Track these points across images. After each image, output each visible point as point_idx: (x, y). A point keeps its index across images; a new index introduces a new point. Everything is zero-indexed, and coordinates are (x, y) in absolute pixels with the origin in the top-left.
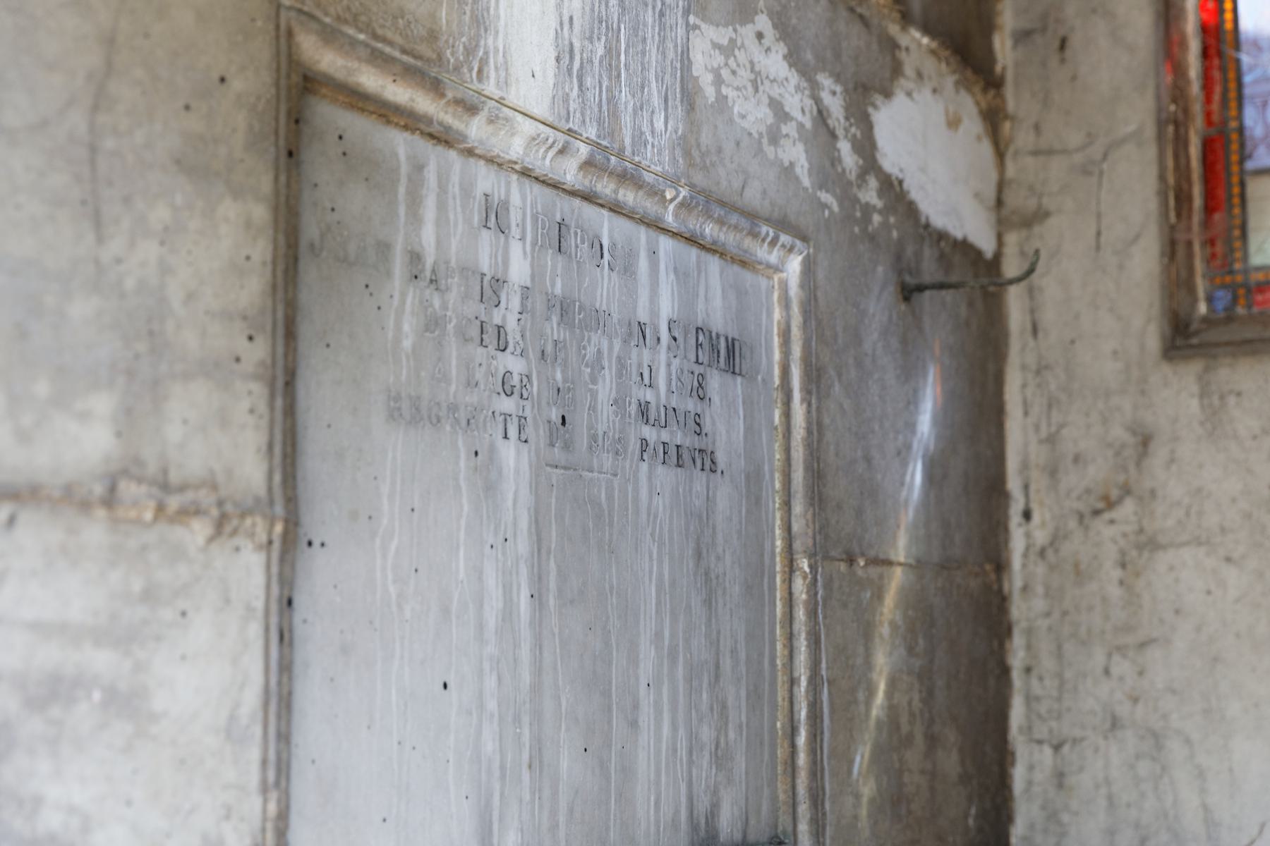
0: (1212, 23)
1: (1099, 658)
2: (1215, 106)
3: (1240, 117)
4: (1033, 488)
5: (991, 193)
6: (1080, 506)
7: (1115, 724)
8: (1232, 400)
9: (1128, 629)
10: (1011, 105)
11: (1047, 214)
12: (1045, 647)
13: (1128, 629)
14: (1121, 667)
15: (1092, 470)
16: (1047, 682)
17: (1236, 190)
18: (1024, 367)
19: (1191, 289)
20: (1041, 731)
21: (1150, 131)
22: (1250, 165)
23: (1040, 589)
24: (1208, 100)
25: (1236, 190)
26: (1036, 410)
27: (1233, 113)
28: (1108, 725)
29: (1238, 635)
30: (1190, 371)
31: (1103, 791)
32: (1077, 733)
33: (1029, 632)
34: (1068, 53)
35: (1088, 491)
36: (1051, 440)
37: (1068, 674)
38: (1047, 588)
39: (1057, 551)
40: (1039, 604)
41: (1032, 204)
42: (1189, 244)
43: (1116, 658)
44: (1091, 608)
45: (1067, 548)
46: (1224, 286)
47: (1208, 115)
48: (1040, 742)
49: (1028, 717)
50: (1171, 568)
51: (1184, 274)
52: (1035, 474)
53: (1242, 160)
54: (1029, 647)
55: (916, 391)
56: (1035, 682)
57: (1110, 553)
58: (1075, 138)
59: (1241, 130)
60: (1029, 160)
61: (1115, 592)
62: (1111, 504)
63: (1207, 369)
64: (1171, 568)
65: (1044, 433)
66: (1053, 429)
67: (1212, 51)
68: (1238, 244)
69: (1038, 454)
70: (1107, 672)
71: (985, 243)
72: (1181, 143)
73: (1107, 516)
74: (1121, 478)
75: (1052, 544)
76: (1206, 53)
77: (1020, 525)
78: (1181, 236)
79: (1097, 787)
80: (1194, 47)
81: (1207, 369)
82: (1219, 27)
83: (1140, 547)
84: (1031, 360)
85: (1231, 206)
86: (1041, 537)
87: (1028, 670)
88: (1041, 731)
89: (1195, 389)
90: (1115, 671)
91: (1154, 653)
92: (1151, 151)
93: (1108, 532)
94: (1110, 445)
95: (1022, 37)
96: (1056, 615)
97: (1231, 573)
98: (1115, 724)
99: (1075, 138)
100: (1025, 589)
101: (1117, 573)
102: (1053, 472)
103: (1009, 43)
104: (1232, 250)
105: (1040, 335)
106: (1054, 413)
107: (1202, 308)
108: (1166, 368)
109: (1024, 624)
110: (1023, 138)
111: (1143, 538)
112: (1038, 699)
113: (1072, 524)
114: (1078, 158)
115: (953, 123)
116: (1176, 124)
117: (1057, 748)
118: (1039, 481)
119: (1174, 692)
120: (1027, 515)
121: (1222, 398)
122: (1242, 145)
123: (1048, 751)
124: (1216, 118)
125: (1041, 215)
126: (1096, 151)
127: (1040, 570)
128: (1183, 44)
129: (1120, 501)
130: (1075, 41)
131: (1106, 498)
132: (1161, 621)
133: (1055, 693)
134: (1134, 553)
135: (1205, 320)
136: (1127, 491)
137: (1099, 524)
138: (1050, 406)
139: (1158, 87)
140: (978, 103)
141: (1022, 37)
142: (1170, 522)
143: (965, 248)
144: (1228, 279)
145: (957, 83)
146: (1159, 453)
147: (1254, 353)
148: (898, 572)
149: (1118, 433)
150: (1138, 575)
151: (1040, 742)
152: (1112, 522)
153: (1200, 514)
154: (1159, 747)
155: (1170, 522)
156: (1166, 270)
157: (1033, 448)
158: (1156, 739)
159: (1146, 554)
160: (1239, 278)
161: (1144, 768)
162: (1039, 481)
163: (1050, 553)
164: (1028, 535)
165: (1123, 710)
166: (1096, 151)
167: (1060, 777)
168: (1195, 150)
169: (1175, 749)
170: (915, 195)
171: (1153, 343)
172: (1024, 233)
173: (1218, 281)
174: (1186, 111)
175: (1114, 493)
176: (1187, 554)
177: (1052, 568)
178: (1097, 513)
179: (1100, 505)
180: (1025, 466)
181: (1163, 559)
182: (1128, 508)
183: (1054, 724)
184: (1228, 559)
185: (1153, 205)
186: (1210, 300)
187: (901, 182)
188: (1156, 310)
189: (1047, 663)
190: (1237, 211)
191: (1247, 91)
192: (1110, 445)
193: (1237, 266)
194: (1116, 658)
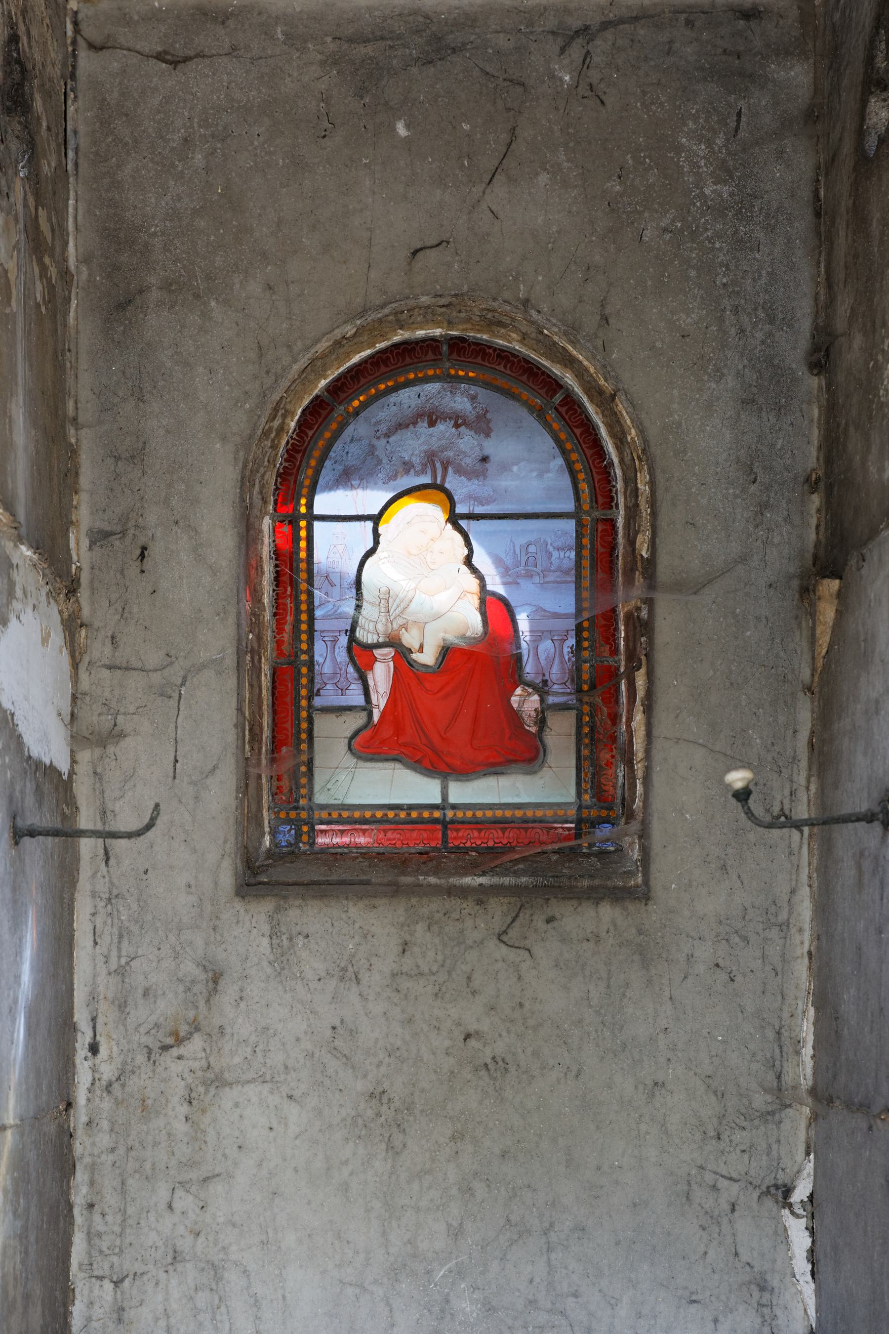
0: (287, 549)
1: (163, 1193)
2: (286, 637)
3: (310, 651)
4: (100, 1020)
5: (67, 710)
6: (145, 1040)
7: (176, 1257)
8: (300, 941)
9: (192, 1164)
10: (86, 612)
11: (122, 735)
12: (108, 1183)
13: (192, 1164)
14: (184, 1201)
15: (161, 1004)
16: (109, 1218)
17: (304, 725)
18: (94, 894)
19: (260, 824)
20: (102, 1267)
21: (230, 661)
22: (318, 702)
23: (105, 1125)
24: (280, 628)
25: (304, 725)
26: (105, 941)
27: (304, 646)
28: (169, 1259)
29: (296, 1170)
30: (263, 908)
31: (162, 1323)
32: (139, 1267)
33: (93, 1168)
34: (148, 564)
35: (157, 1026)
36: (121, 972)
37: (130, 1211)
38: (113, 1123)
39: (123, 1086)
40: (104, 1140)
41: (106, 722)
42: (259, 777)
43: (180, 1193)
44: (156, 1144)
45: (134, 1083)
46: (289, 821)
47: (279, 643)
48: (101, 1278)
49: (89, 1254)
50: (237, 1105)
51: (254, 808)
52: (103, 1007)
53: (310, 698)
54: (92, 1183)
55: (20, 939)
56: (97, 1218)
57: (178, 1088)
58: (154, 658)
59: (311, 664)
60: (105, 673)
61: (181, 1128)
62: (179, 1041)
63: (278, 910)
64: (237, 1105)
65: (113, 965)
66: (123, 961)
67: (286, 578)
68: (304, 781)
69: (107, 986)
70: (170, 1207)
71: (63, 766)
72: (257, 670)
73: (175, 1052)
74: (191, 1014)
75: (119, 1079)
76: (278, 579)
77: (86, 1059)
78: (253, 771)
79: (157, 1319)
80: (268, 569)
81: (278, 910)
82: (293, 555)
83: (207, 1084)
84: (102, 887)
85: (299, 741)
86: (107, 1072)
87: (91, 1206)
88: (102, 1267)
89: (266, 929)
90: (177, 1205)
91: (217, 1188)
92: (231, 682)
93: (177, 1067)
94: (180, 980)
95: (99, 537)
96: (121, 1150)
97: (293, 1111)
98: (176, 1257)
99: (154, 658)
100: (89, 1123)
101: (184, 1109)
102: (122, 1006)
103: (85, 543)
104: (298, 787)
105: (112, 862)
106: (125, 943)
107: (267, 841)
108: (239, 905)
109: (87, 1160)
110: (100, 650)
111: (210, 1075)
112: (99, 1235)
113: (140, 1059)
114: (156, 678)
115: (45, 640)
116: (252, 651)
117: (117, 1283)
118: (107, 1014)
119: (234, 1225)
120: (94, 1049)
121: (291, 939)
122: (312, 681)
123: (108, 1286)
124: (286, 648)
125: (115, 735)
126: (175, 674)
127: (106, 1105)
128: (259, 568)
129: (189, 1036)
130: (156, 551)
131: (175, 1034)
132: (225, 1156)
133: (117, 1229)
134: (201, 1089)
135: (269, 854)
136: (195, 1027)
137: (167, 1060)
138: (121, 936)
139: (239, 614)
140: (61, 612)
141: (99, 537)
142: (237, 1060)
143: (51, 770)
144: (293, 814)
145: (49, 594)
146: (229, 991)
147: (322, 896)
148: (9, 1134)
149: (189, 968)
150: (204, 1111)
151: (101, 1278)
152: (180, 1058)
153: (266, 1051)
154: (218, 1279)
155: (237, 1060)
156: (240, 806)
157: (102, 979)
158: (216, 1270)
159: (212, 1091)
160: (304, 815)
161: (202, 1299)
162: (107, 1014)
163: (116, 1086)
164: (94, 1069)
165: (185, 1244)
166: (175, 674)
167: (119, 1312)
168: (265, 681)
169: (232, 1276)
170: (21, 729)
171: (227, 879)
172: (98, 751)
173: (282, 815)
174: (259, 638)
175: (183, 1030)
176: (251, 1091)
177: (118, 1103)
178: (165, 1048)
179: (170, 1041)
180: (93, 998)
181: (229, 1096)
182: (197, 1043)
183: (115, 1259)
184: (290, 1097)
185: (231, 737)
186: (274, 833)
187: (13, 715)
188: (230, 847)
189: (111, 1199)
190: (304, 746)
191: (318, 626)
192: (180, 980)
193: (302, 802)
194: (180, 1193)
